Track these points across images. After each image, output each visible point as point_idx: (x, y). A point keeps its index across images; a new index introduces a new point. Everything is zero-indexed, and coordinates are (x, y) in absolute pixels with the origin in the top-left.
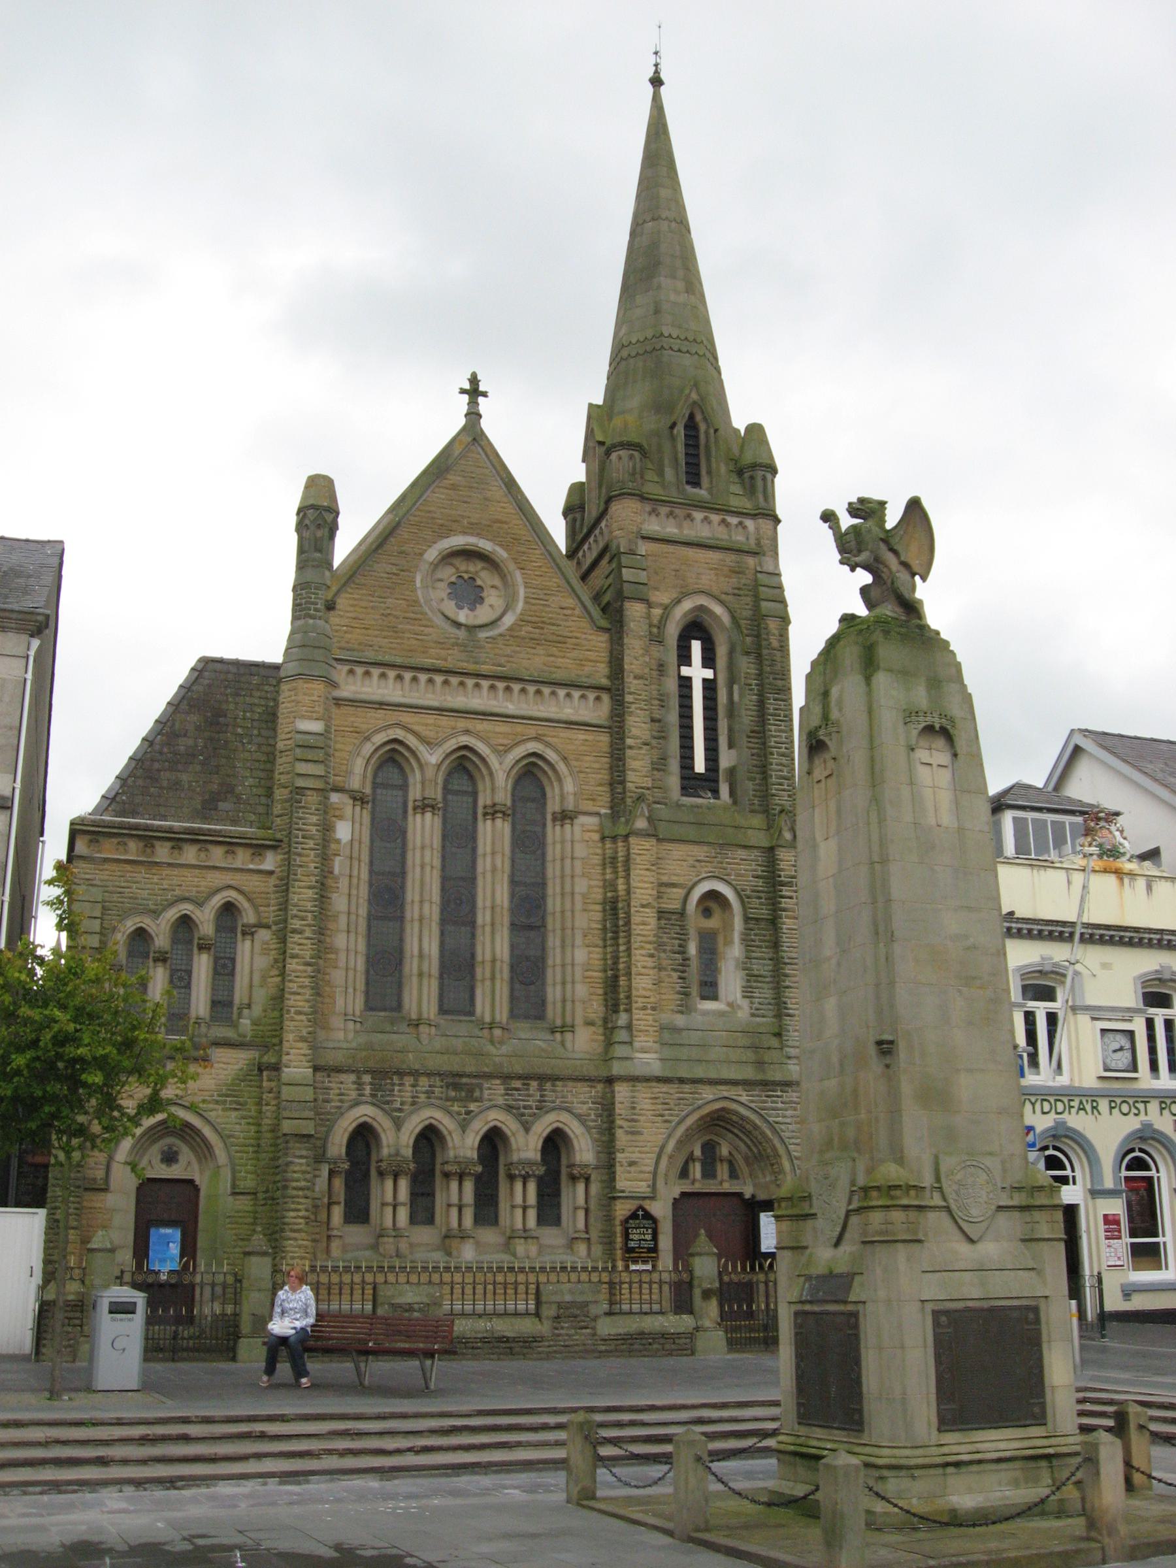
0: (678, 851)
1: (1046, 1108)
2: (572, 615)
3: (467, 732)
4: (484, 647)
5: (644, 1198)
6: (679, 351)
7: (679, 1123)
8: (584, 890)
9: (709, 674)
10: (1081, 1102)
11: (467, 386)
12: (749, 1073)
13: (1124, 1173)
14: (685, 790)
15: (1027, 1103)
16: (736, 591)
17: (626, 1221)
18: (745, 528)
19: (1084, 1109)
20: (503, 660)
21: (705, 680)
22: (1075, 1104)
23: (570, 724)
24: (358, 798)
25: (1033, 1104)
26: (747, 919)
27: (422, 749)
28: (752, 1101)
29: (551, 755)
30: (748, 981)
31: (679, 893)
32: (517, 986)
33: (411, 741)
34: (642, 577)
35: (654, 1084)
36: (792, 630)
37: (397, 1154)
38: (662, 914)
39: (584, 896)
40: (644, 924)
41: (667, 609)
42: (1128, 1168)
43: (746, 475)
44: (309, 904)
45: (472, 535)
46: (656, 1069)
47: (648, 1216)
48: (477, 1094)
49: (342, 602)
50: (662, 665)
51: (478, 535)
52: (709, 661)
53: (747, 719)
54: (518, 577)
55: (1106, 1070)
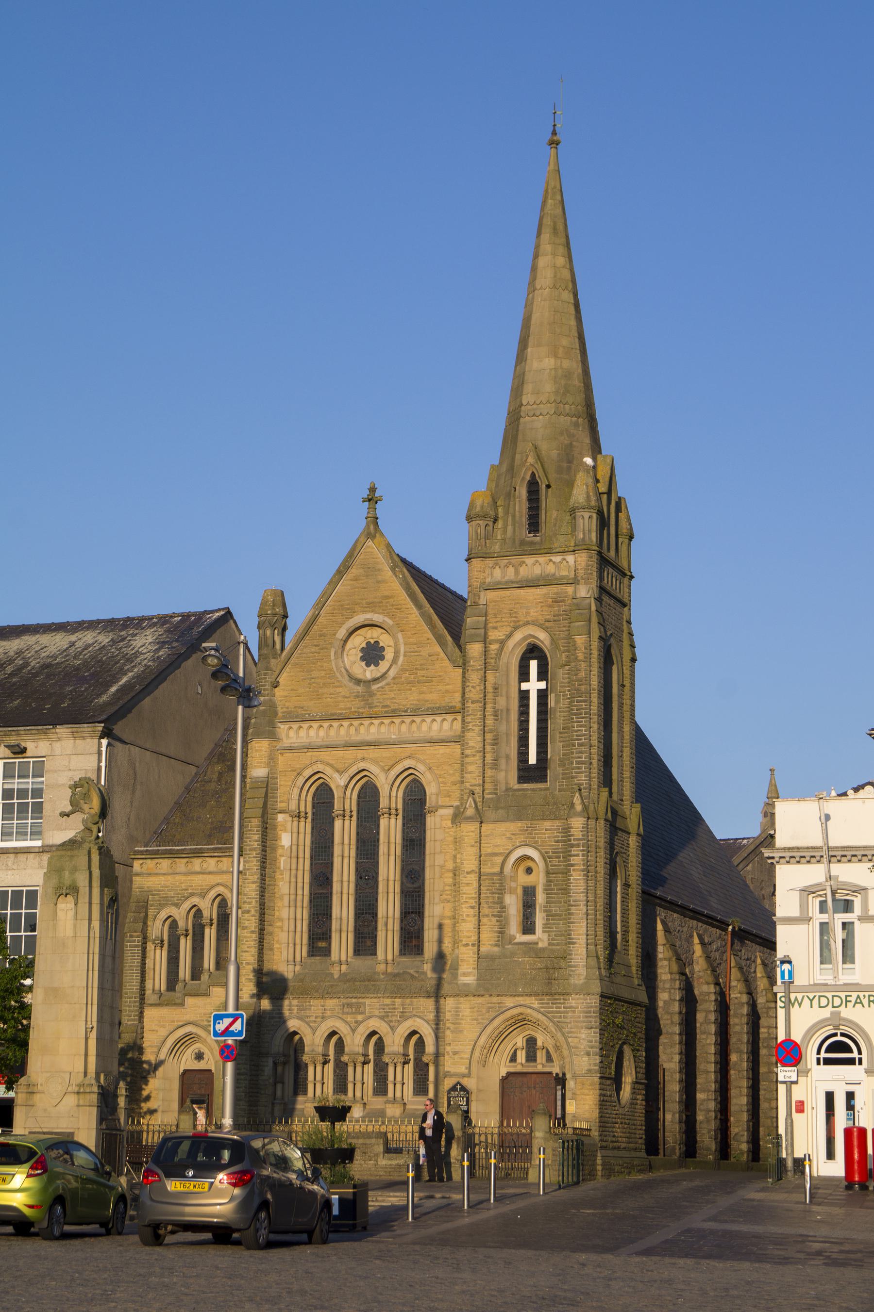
1: (824, 1002)
3: (363, 759)
5: (464, 1076)
6: (534, 415)
9: (542, 685)
13: (823, 1055)
14: (522, 779)
15: (806, 998)
16: (556, 618)
17: (449, 1092)
19: (861, 1002)
23: (432, 742)
25: (811, 1001)
28: (542, 1008)
30: (548, 920)
31: (499, 860)
37: (313, 1051)
39: (442, 867)
41: (502, 643)
42: (827, 1051)
45: (369, 612)
47: (463, 1089)
48: (362, 1009)
49: (282, 680)
52: (542, 675)
54: (400, 635)
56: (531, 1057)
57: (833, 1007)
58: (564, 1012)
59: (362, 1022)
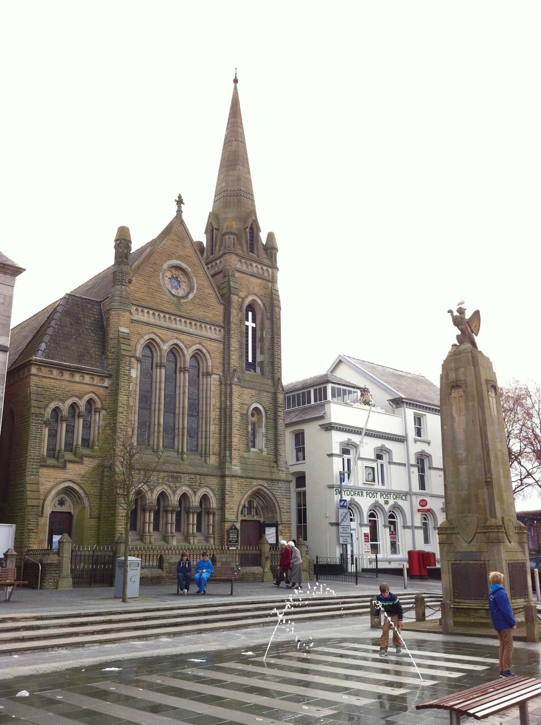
0: (247, 391)
2: (212, 297)
4: (182, 306)
5: (234, 522)
7: (245, 494)
8: (214, 403)
10: (358, 492)
11: (177, 199)
12: (267, 476)
18: (268, 272)
19: (359, 494)
20: (188, 311)
21: (252, 327)
22: (356, 492)
24: (138, 360)
26: (267, 418)
27: (161, 343)
28: (268, 486)
29: (204, 351)
30: (267, 441)
31: (246, 407)
32: (188, 438)
33: (158, 340)
34: (237, 286)
35: (239, 479)
36: (282, 312)
38: (242, 415)
40: (236, 418)
43: (269, 251)
44: (126, 402)
46: (239, 473)
48: (179, 479)
50: (241, 321)
51: (181, 261)
53: (267, 344)
55: (366, 481)
56: (249, 513)
57: (351, 495)
58: (277, 490)
59: (179, 487)
